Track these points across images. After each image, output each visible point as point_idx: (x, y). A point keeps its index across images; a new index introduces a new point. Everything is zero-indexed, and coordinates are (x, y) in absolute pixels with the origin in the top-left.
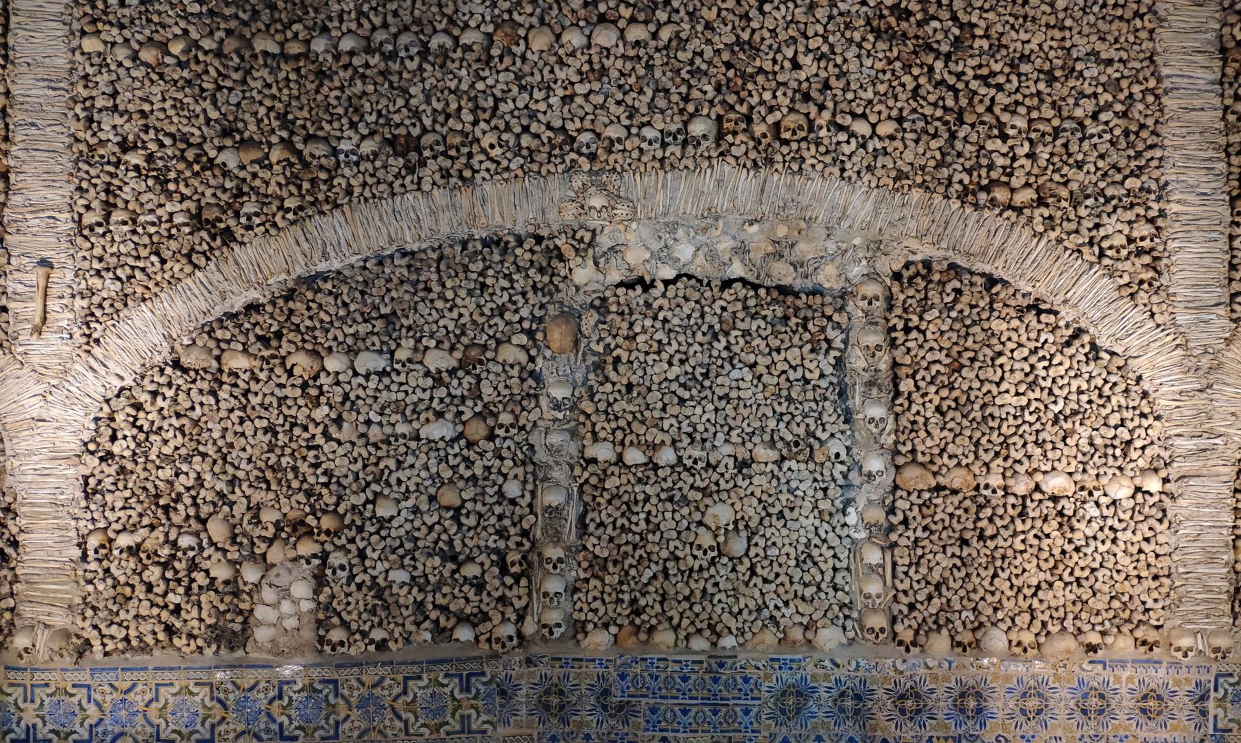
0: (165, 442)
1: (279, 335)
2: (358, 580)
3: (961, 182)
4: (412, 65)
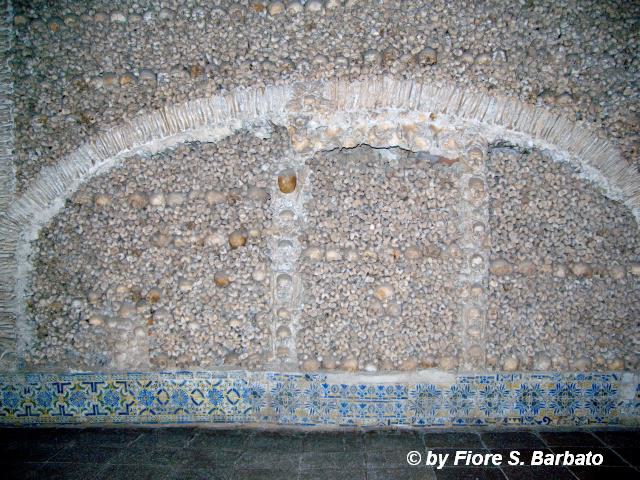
0: (64, 247)
1: (124, 184)
2: (172, 326)
3: (527, 91)
4: (201, 26)
